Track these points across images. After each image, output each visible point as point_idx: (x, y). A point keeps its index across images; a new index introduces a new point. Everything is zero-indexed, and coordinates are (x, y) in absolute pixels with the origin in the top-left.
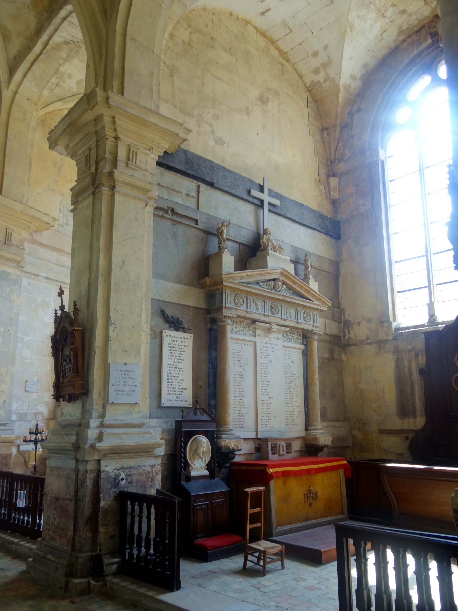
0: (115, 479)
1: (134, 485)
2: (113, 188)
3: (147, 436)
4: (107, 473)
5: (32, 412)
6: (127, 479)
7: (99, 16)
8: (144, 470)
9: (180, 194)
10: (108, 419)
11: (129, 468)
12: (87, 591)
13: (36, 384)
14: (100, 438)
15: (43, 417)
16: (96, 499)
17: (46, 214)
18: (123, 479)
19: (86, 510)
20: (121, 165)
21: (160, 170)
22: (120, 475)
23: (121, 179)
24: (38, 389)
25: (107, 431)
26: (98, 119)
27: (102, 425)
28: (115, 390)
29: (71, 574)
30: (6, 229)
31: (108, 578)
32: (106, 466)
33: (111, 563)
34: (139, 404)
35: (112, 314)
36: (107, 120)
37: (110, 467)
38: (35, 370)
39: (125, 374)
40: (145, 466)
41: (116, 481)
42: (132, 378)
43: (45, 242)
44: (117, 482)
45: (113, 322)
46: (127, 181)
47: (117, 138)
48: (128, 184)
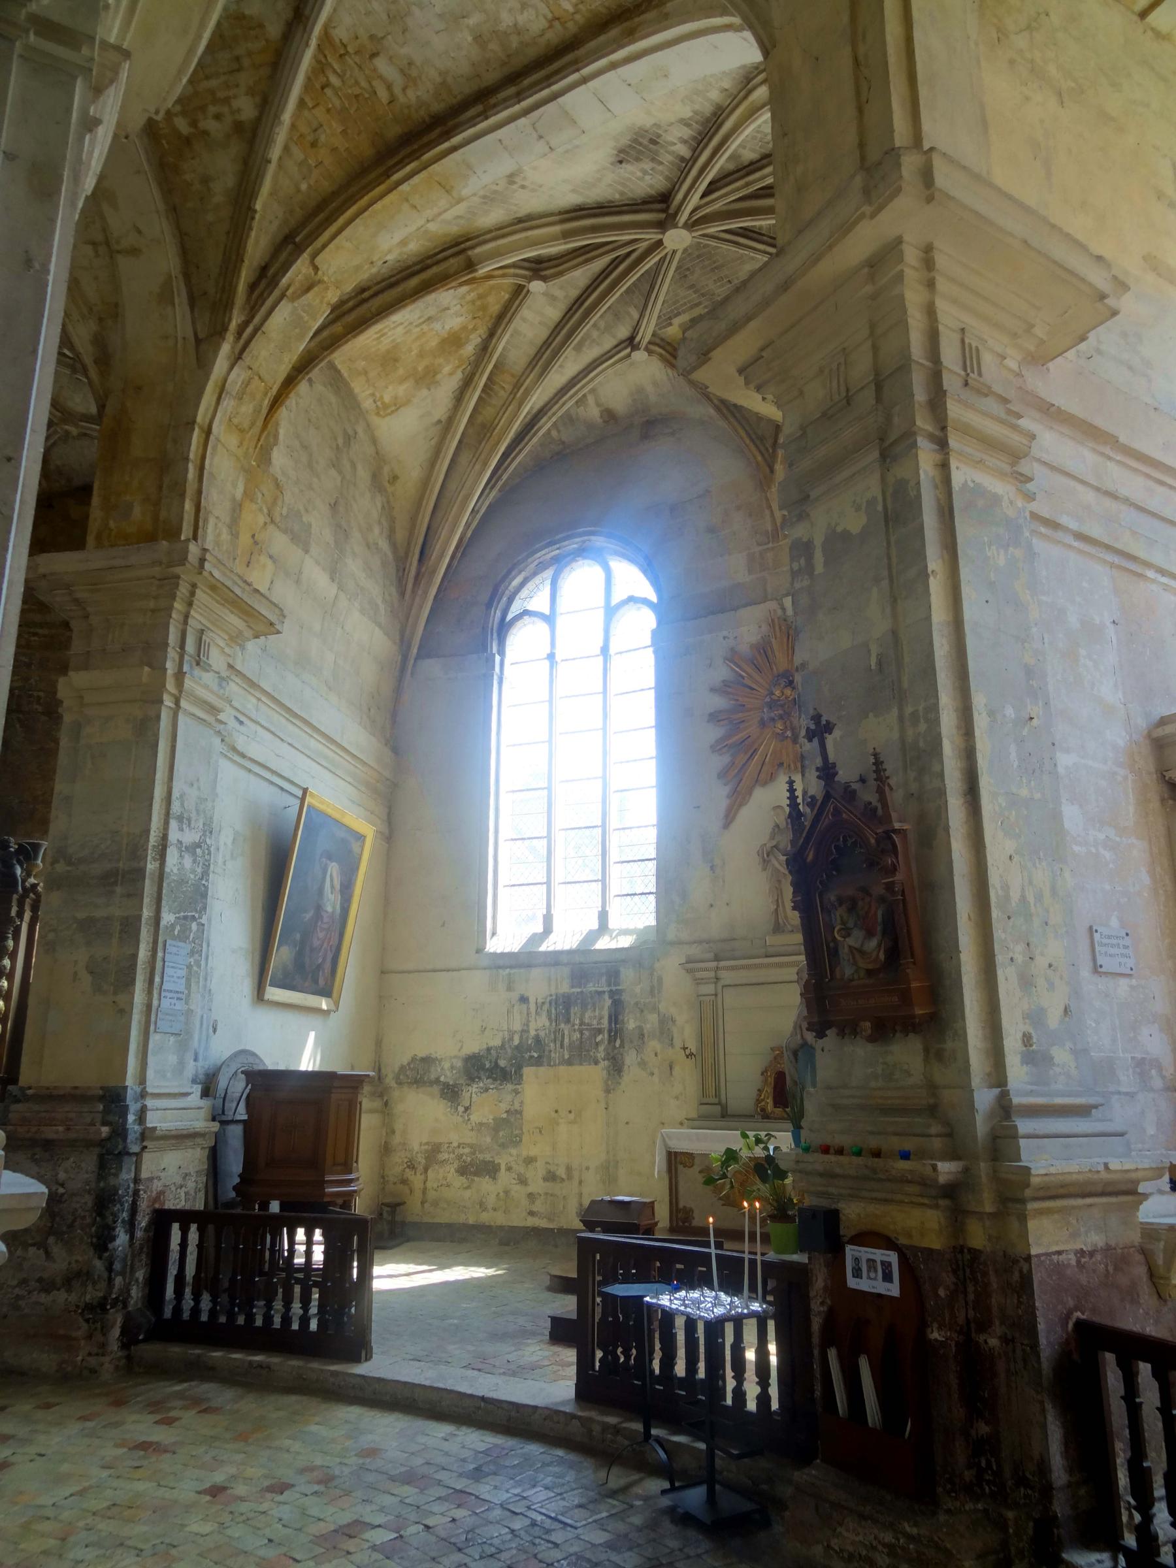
5: (1129, 1056)
13: (1121, 942)
15: (1163, 1077)
17: (1099, 258)
24: (1131, 963)
30: (963, 330)
38: (1107, 887)
43: (1060, 401)
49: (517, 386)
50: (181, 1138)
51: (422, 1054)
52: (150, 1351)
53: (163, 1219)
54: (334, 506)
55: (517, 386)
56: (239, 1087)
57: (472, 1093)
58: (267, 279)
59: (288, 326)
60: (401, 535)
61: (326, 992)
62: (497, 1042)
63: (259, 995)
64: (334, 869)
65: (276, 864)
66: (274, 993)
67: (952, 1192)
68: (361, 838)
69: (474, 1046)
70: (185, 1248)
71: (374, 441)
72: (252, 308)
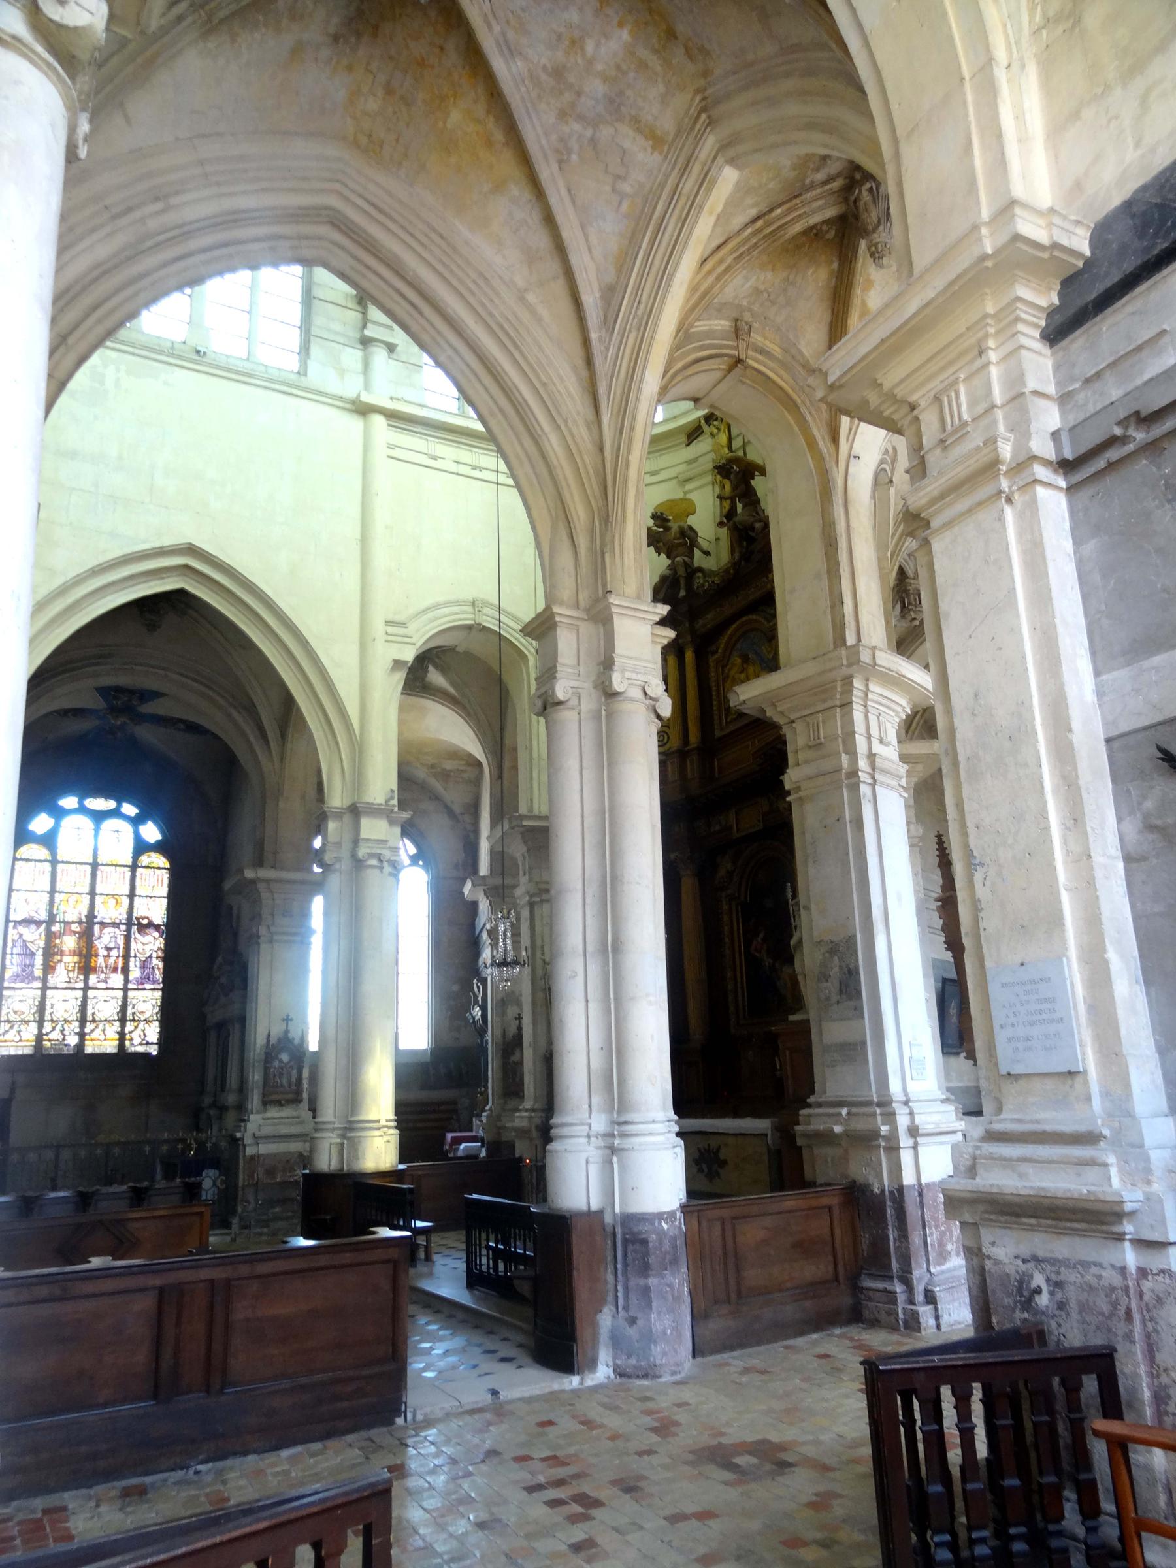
0: (1021, 1282)
1: (1074, 1315)
3: (1092, 1174)
4: (997, 1262)
6: (1052, 1293)
8: (1099, 1277)
9: (1166, 339)
11: (1053, 1262)
18: (1038, 1291)
21: (1078, 341)
22: (1031, 1276)
23: (924, 501)
28: (1010, 1040)
32: (993, 1244)
34: (1085, 1072)
35: (972, 842)
39: (1026, 992)
40: (1100, 1265)
42: (1046, 1000)
44: (1026, 1293)
45: (977, 861)
46: (936, 493)
48: (942, 496)
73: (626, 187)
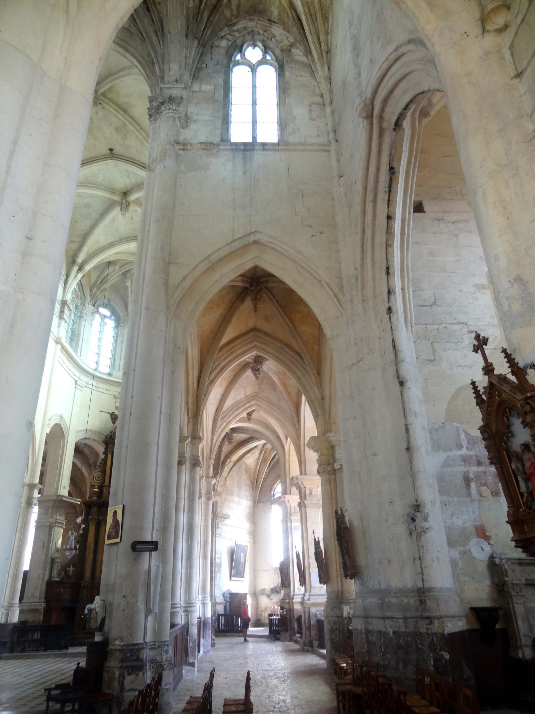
2: (305, 507)
7: (296, 438)
10: (312, 593)
12: (308, 651)
14: (309, 600)
16: (310, 621)
19: (307, 625)
20: (308, 497)
25: (311, 597)
26: (298, 483)
27: (310, 595)
29: (304, 646)
31: (315, 648)
33: (316, 643)
36: (300, 483)
37: (313, 610)
41: (316, 615)
47: (305, 487)
49: (270, 452)
50: (220, 603)
51: (263, 588)
52: (218, 634)
53: (219, 615)
54: (238, 484)
55: (270, 452)
56: (228, 595)
57: (272, 596)
58: (224, 463)
59: (227, 469)
60: (252, 478)
61: (243, 577)
62: (276, 585)
63: (231, 580)
64: (242, 554)
65: (232, 555)
66: (233, 578)
67: (289, 603)
68: (247, 546)
69: (272, 586)
70: (222, 619)
71: (245, 464)
72: (222, 468)
73: (236, 398)
